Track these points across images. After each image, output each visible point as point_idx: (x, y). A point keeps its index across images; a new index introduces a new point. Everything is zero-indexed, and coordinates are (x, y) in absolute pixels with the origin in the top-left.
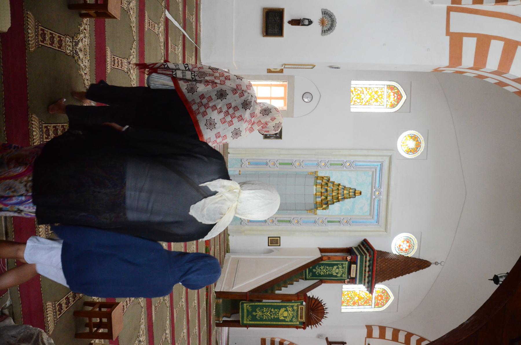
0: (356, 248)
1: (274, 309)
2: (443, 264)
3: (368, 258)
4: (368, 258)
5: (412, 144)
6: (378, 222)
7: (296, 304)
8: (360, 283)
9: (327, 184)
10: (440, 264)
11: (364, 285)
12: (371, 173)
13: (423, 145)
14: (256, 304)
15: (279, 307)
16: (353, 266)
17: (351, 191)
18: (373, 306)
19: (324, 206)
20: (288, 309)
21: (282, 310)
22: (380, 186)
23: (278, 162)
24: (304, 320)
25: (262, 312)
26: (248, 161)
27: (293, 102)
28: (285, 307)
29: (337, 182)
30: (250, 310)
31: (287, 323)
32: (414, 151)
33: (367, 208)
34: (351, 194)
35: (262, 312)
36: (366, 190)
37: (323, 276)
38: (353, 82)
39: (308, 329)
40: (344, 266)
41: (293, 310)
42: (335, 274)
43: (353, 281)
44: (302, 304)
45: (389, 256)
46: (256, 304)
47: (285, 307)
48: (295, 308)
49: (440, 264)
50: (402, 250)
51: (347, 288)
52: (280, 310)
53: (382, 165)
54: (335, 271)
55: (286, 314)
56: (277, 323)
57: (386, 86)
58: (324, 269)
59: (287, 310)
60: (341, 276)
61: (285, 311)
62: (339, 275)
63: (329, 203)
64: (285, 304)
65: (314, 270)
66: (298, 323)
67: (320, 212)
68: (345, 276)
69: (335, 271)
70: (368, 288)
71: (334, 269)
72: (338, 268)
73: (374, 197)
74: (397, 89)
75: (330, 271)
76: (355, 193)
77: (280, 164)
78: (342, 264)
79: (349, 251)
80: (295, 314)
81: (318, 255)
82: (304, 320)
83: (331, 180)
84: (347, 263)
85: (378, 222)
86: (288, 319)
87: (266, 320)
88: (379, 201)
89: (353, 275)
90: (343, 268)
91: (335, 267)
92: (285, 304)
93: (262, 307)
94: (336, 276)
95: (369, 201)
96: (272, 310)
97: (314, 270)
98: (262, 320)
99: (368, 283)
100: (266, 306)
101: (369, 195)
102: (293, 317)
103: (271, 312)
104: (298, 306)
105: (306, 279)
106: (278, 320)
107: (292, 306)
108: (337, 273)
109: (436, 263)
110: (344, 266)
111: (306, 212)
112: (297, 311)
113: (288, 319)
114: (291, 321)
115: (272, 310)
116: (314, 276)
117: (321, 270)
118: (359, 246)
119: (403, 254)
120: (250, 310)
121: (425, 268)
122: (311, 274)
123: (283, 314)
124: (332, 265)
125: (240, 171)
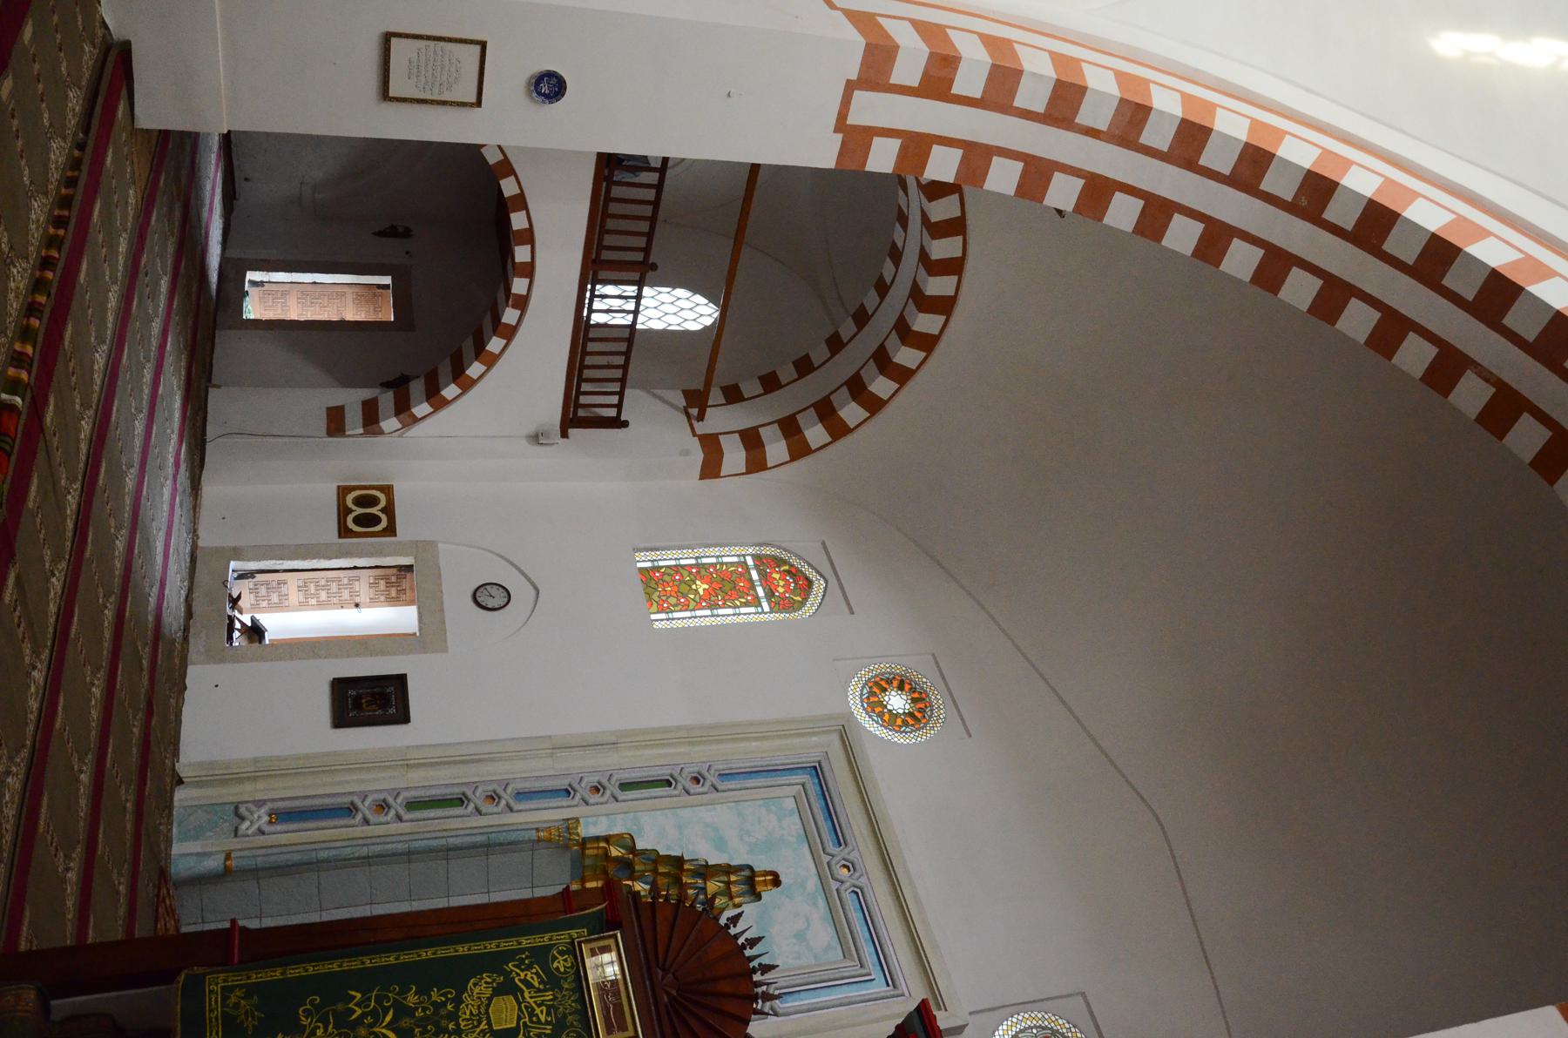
1: (423, 991)
5: (897, 702)
7: (562, 937)
12: (790, 804)
13: (937, 699)
14: (294, 972)
15: (457, 975)
17: (733, 878)
20: (519, 976)
21: (479, 988)
22: (840, 841)
23: (399, 800)
26: (269, 805)
27: (442, 610)
28: (494, 963)
30: (250, 1023)
32: (916, 718)
33: (822, 935)
34: (734, 889)
36: (796, 865)
38: (639, 556)
41: (552, 981)
46: (294, 972)
47: (494, 963)
48: (560, 964)
52: (462, 989)
53: (817, 771)
57: (750, 561)
59: (508, 988)
61: (499, 991)
64: (491, 946)
73: (834, 885)
74: (785, 562)
77: (412, 805)
80: (571, 1003)
83: (640, 845)
85: (891, 981)
88: (858, 892)
92: (491, 946)
93: (333, 989)
95: (822, 903)
96: (412, 999)
100: (366, 980)
101: (813, 883)
103: (402, 1011)
107: (541, 956)
115: (412, 999)
120: (250, 1023)
125: (228, 856)
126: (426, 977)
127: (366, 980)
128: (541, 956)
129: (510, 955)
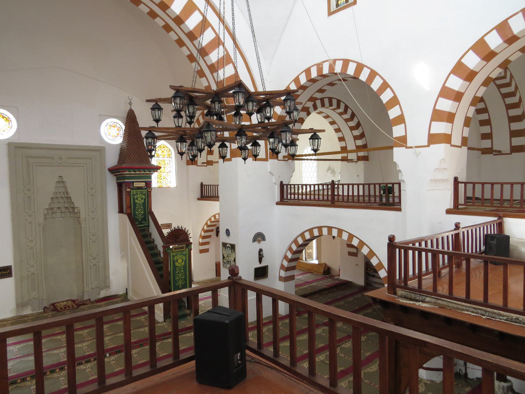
0: (117, 179)
1: (176, 271)
2: (130, 98)
3: (128, 172)
4: (128, 172)
6: (91, 159)
7: (171, 254)
8: (150, 177)
9: (52, 209)
10: (130, 100)
11: (152, 174)
14: (172, 286)
15: (175, 267)
16: (136, 185)
18: (170, 159)
19: (76, 211)
20: (176, 259)
21: (177, 264)
22: (52, 158)
24: (184, 245)
25: (179, 280)
28: (174, 262)
29: (49, 201)
31: (187, 259)
32: (8, 119)
35: (179, 280)
37: (145, 211)
39: (191, 240)
40: (135, 193)
41: (176, 255)
42: (143, 200)
43: (148, 184)
44: (172, 249)
45: (125, 145)
46: (172, 286)
47: (174, 262)
48: (174, 254)
49: (130, 100)
50: (118, 134)
51: (154, 184)
54: (139, 202)
55: (180, 261)
56: (187, 266)
58: (138, 211)
59: (177, 261)
60: (144, 195)
62: (144, 197)
63: (72, 206)
65: (140, 220)
66: (187, 250)
67: (82, 215)
68: (145, 191)
69: (139, 202)
70: (154, 171)
71: (139, 202)
72: (137, 199)
75: (140, 206)
76: (61, 182)
78: (134, 195)
79: (120, 186)
80: (180, 253)
81: (125, 217)
82: (184, 245)
84: (132, 191)
85: (91, 159)
86: (184, 258)
87: (186, 276)
89: (143, 185)
90: (137, 194)
91: (136, 201)
94: (145, 200)
97: (140, 220)
98: (185, 280)
99: (150, 171)
100: (174, 278)
102: (182, 254)
103: (178, 273)
104: (173, 252)
105: (148, 226)
106: (185, 267)
108: (142, 199)
109: (130, 104)
110: (135, 193)
111: (83, 229)
112: (178, 252)
113: (184, 258)
114: (185, 255)
116: (145, 219)
117: (140, 213)
118: (115, 175)
119: (122, 133)
121: (135, 116)
122: (143, 222)
123: (180, 263)
124: (135, 203)
126: (175, 270)
127: (174, 278)
128: (173, 256)
129: (173, 260)
